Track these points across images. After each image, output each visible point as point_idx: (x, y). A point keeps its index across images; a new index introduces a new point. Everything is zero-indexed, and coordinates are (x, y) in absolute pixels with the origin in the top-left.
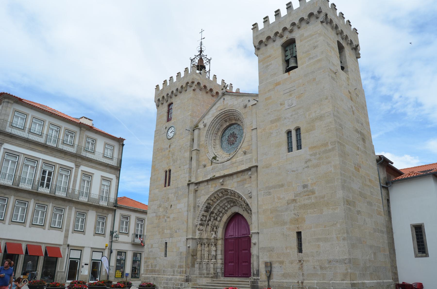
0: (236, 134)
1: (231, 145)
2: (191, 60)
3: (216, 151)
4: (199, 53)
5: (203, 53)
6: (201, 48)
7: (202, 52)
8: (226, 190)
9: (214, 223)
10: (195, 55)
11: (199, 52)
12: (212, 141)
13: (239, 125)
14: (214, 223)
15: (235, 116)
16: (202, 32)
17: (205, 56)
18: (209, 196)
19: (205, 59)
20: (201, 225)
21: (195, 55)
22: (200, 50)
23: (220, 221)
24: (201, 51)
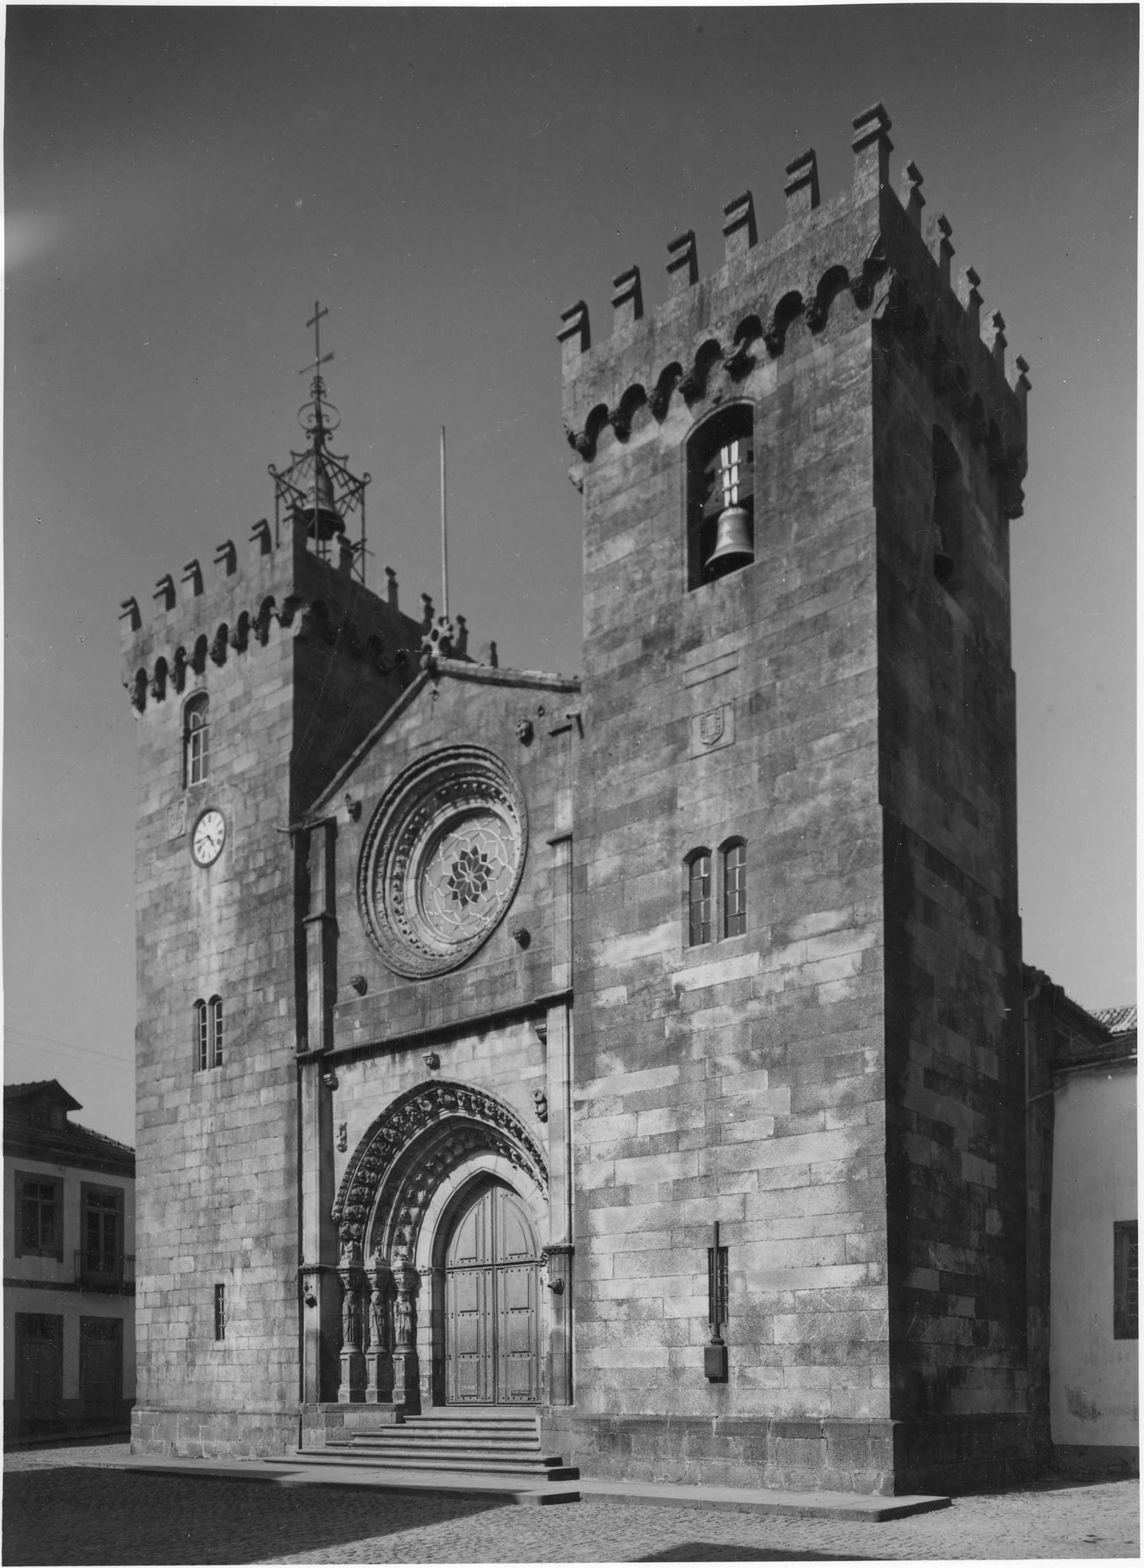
0: (484, 858)
1: (464, 902)
2: (278, 477)
3: (406, 927)
4: (310, 444)
5: (332, 446)
6: (319, 416)
7: (326, 437)
8: (451, 1087)
9: (403, 1212)
10: (293, 454)
11: (312, 436)
12: (388, 881)
13: (496, 815)
14: (403, 1212)
15: (482, 779)
16: (321, 320)
17: (341, 463)
18: (381, 1110)
19: (340, 476)
20: (352, 1218)
21: (293, 454)
22: (314, 424)
23: (425, 1205)
24: (320, 434)
